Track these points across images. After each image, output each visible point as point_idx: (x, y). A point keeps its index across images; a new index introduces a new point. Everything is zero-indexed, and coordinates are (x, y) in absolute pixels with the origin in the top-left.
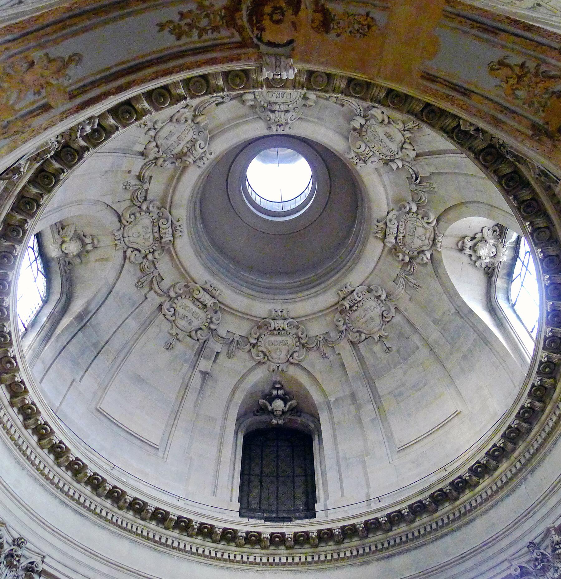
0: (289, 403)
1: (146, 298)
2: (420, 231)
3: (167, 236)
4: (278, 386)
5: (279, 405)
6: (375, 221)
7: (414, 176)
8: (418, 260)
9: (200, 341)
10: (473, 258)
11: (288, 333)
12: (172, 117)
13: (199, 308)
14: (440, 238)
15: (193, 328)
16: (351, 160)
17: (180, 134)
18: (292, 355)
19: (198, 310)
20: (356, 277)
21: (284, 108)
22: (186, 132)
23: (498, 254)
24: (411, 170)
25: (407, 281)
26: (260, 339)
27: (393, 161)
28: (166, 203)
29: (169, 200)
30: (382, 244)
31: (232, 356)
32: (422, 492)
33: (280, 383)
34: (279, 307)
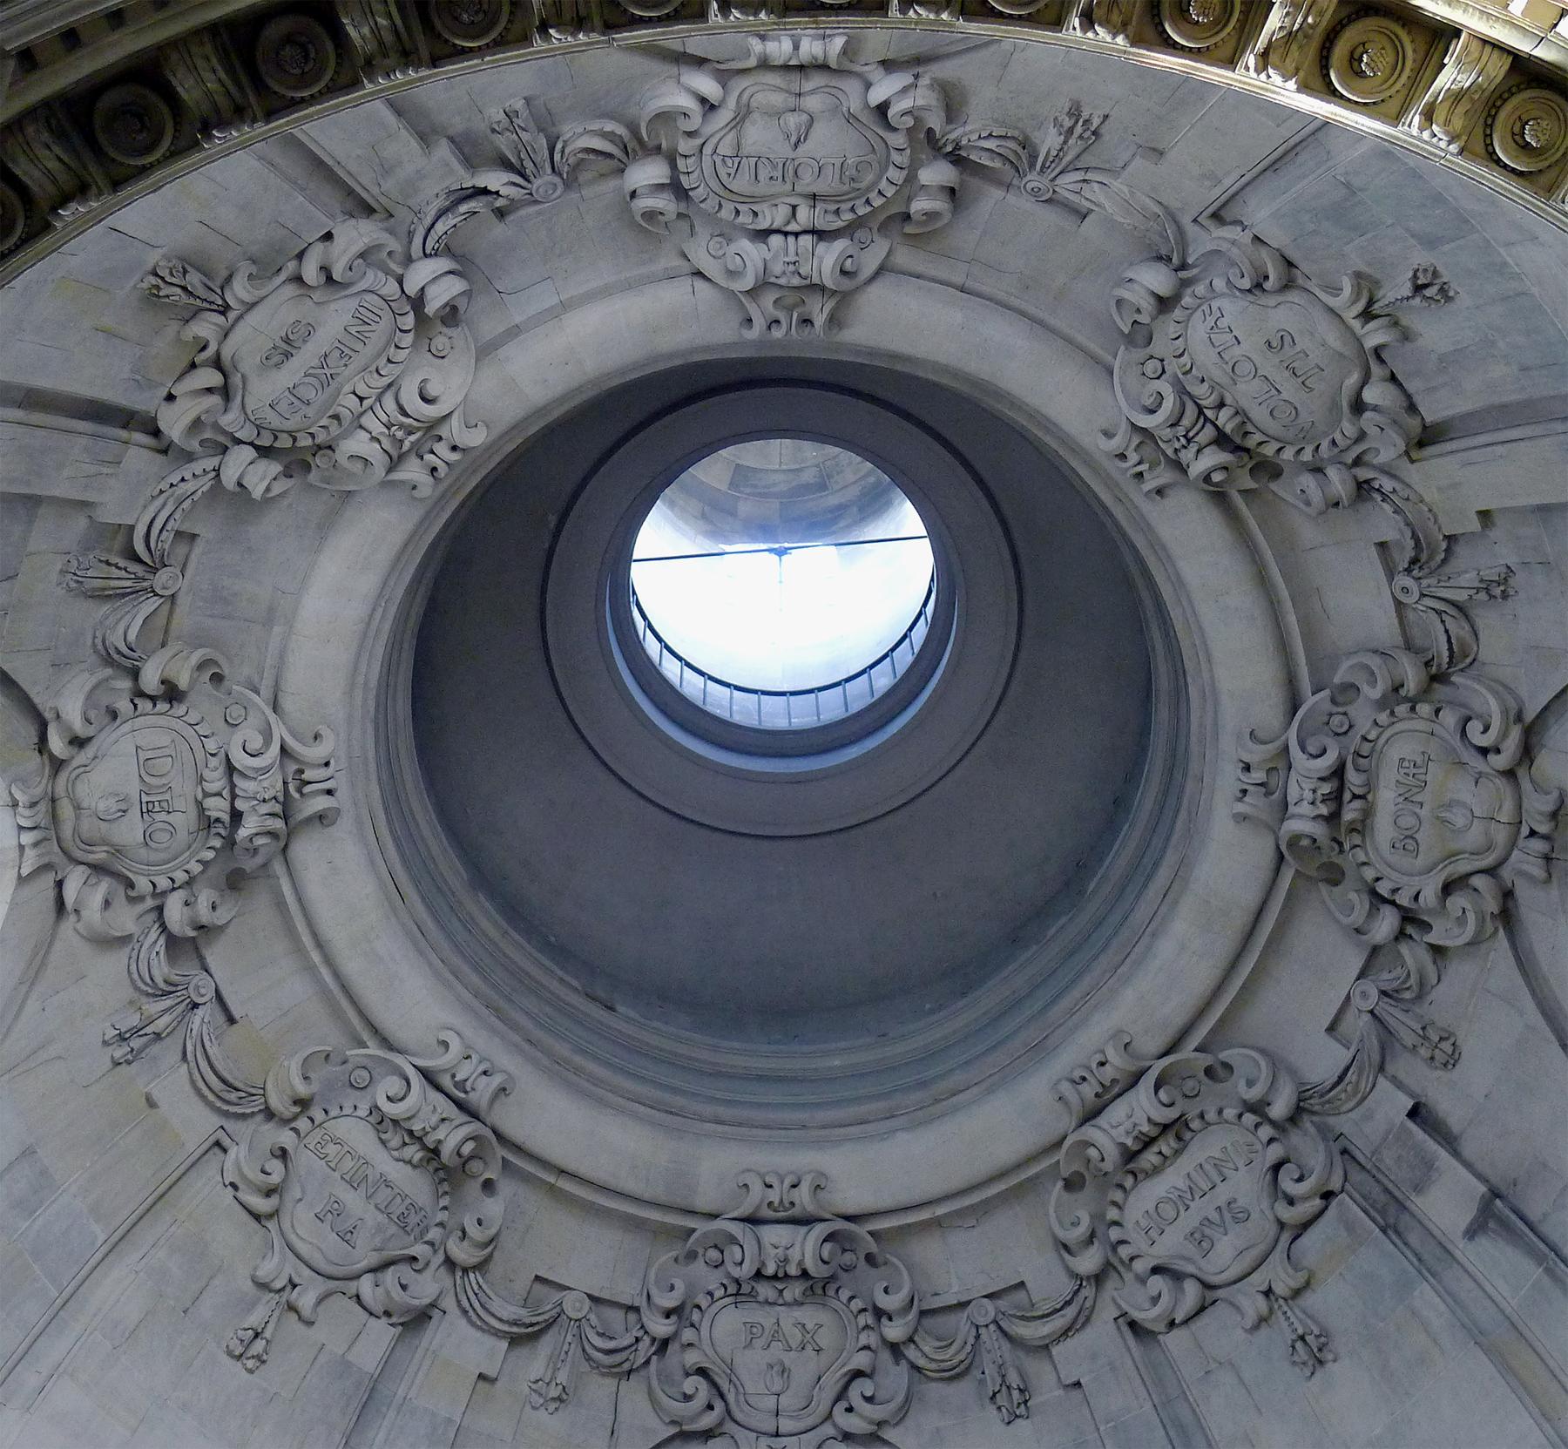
1: (1078, 1384)
3: (795, 1254)
7: (463, 208)
9: (1335, 1184)
11: (1366, 748)
12: (257, 1217)
13: (1177, 1153)
15: (1265, 1204)
16: (443, 470)
17: (337, 1175)
19: (1187, 1163)
22: (332, 1149)
24: (440, 227)
25: (1058, 164)
26: (1383, 889)
27: (418, 303)
28: (673, 1225)
30: (875, 290)
31: (1446, 1046)
34: (1227, 779)
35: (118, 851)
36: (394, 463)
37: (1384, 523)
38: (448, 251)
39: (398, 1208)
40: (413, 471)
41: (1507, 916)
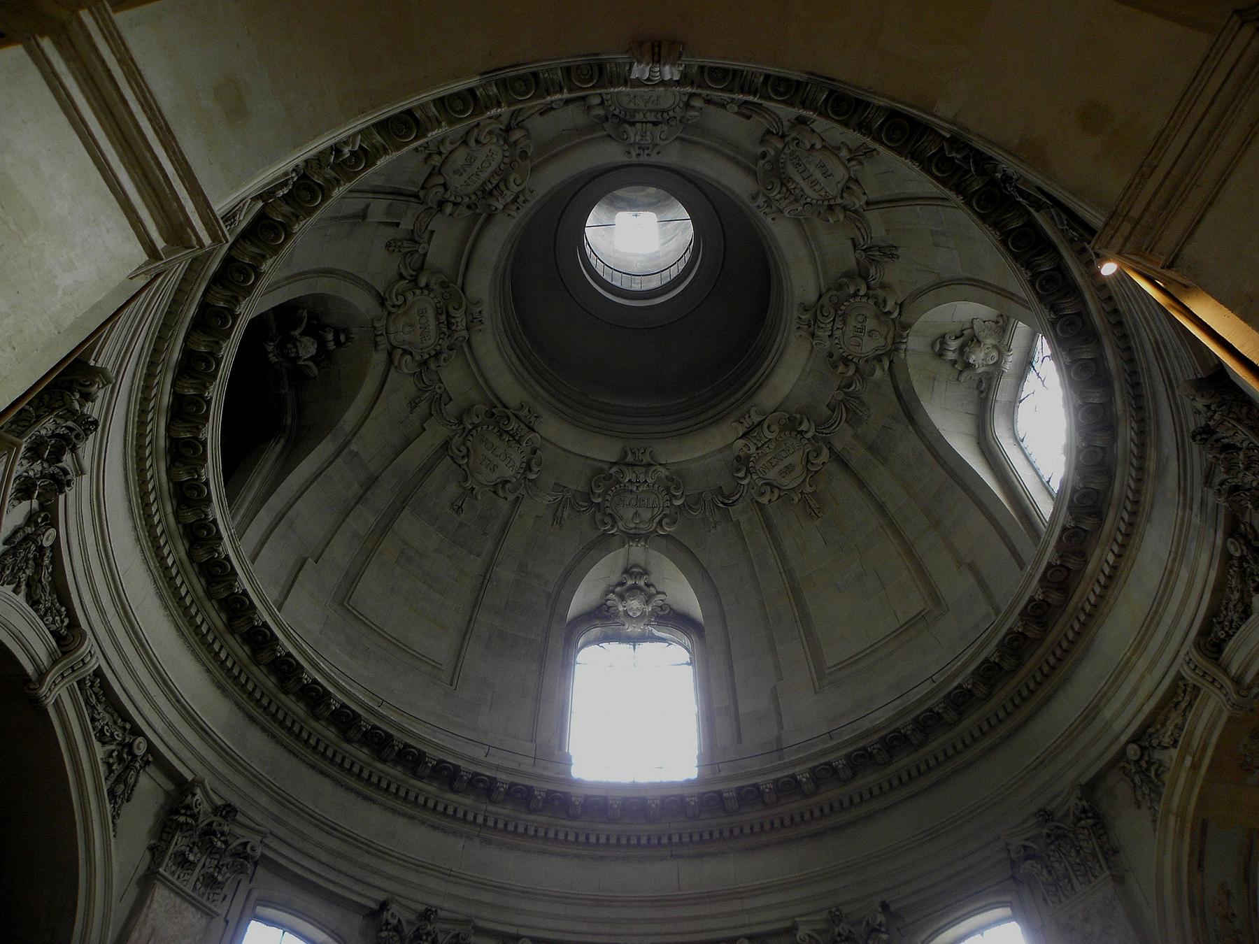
0: (310, 363)
2: (646, 514)
4: (342, 338)
5: (308, 348)
8: (599, 516)
10: (618, 589)
12: (857, 181)
13: (484, 183)
18: (405, 352)
20: (553, 429)
21: (838, 333)
26: (426, 292)
29: (695, 138)
32: (370, 710)
33: (348, 339)
35: (877, 317)
36: (760, 423)
37: (451, 409)
39: (801, 169)
40: (756, 419)
41: (382, 301)
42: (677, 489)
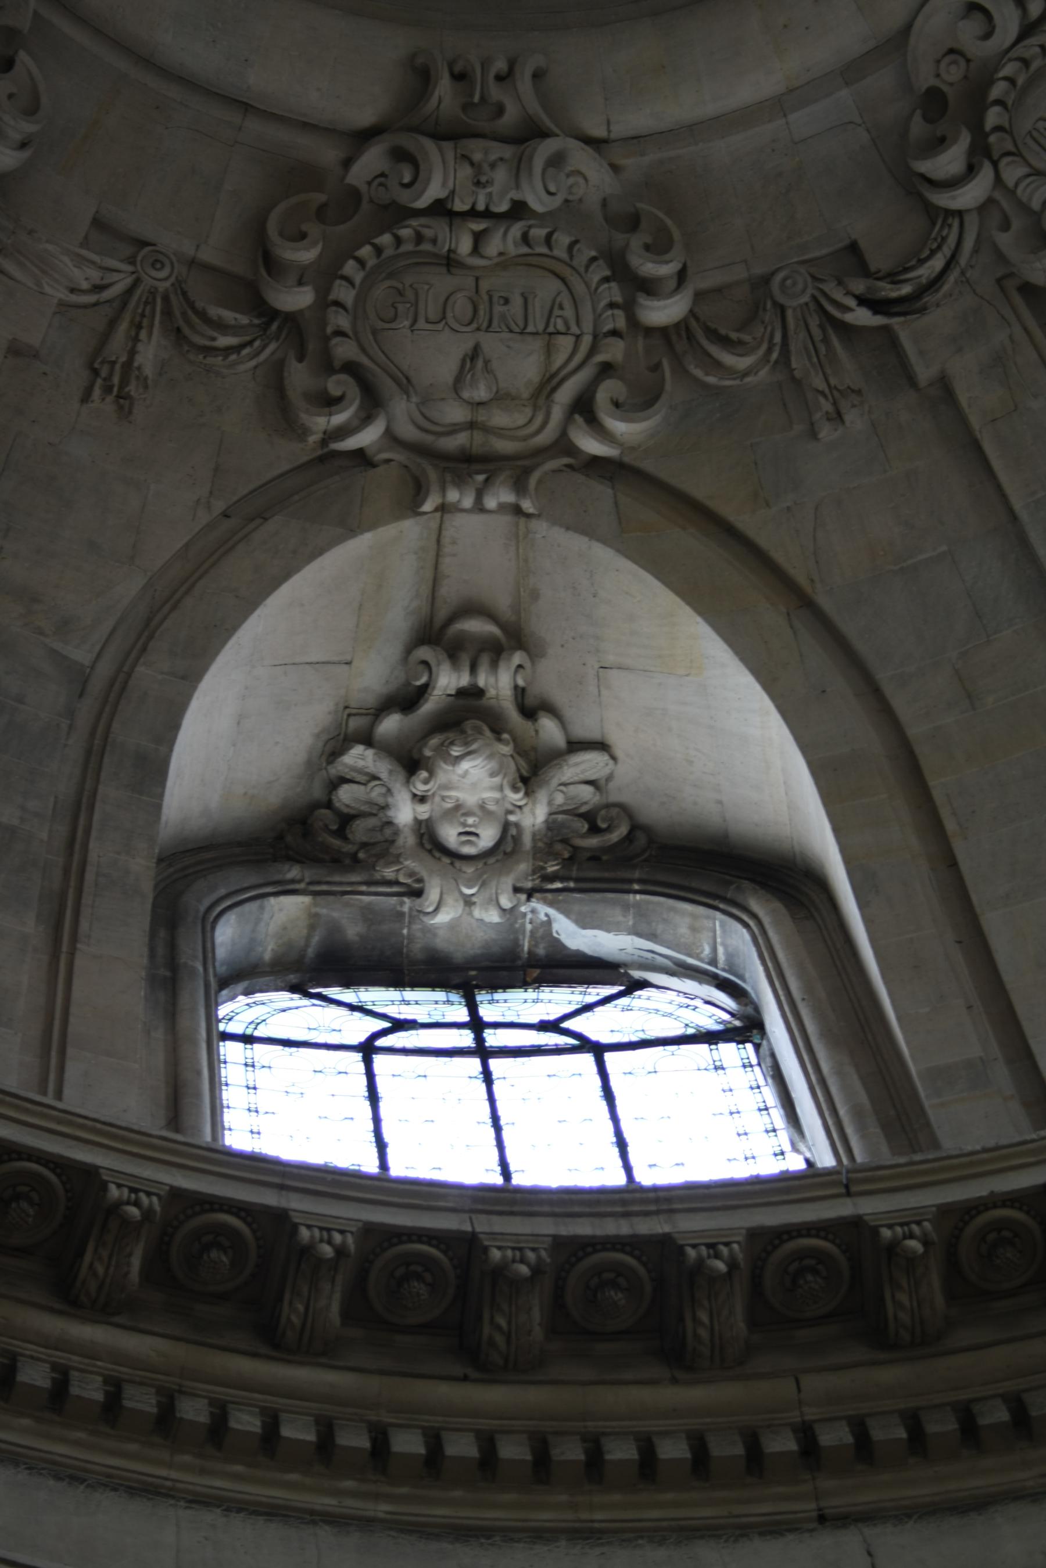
6: (535, 61)
7: (906, 290)
8: (299, 377)
10: (391, 724)
14: (507, 497)
23: (469, 869)
24: (937, 263)
27: (980, 153)
30: (365, 117)
38: (936, 215)
42: (659, 248)
